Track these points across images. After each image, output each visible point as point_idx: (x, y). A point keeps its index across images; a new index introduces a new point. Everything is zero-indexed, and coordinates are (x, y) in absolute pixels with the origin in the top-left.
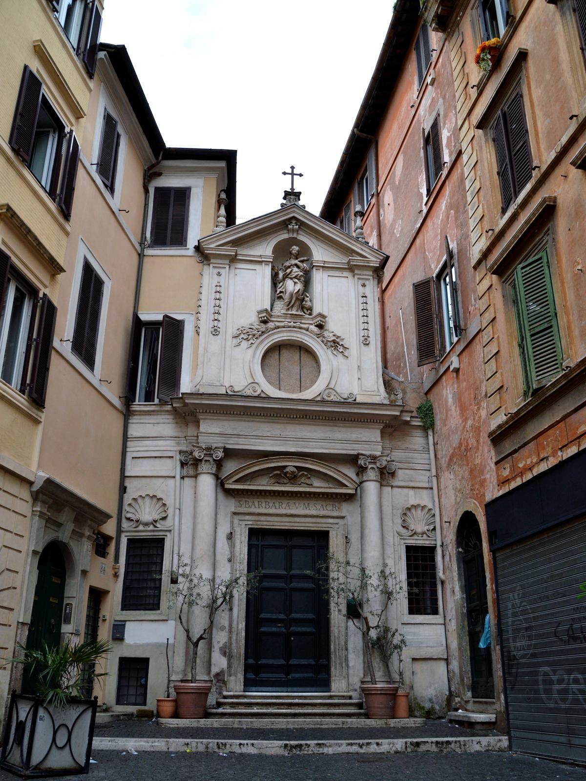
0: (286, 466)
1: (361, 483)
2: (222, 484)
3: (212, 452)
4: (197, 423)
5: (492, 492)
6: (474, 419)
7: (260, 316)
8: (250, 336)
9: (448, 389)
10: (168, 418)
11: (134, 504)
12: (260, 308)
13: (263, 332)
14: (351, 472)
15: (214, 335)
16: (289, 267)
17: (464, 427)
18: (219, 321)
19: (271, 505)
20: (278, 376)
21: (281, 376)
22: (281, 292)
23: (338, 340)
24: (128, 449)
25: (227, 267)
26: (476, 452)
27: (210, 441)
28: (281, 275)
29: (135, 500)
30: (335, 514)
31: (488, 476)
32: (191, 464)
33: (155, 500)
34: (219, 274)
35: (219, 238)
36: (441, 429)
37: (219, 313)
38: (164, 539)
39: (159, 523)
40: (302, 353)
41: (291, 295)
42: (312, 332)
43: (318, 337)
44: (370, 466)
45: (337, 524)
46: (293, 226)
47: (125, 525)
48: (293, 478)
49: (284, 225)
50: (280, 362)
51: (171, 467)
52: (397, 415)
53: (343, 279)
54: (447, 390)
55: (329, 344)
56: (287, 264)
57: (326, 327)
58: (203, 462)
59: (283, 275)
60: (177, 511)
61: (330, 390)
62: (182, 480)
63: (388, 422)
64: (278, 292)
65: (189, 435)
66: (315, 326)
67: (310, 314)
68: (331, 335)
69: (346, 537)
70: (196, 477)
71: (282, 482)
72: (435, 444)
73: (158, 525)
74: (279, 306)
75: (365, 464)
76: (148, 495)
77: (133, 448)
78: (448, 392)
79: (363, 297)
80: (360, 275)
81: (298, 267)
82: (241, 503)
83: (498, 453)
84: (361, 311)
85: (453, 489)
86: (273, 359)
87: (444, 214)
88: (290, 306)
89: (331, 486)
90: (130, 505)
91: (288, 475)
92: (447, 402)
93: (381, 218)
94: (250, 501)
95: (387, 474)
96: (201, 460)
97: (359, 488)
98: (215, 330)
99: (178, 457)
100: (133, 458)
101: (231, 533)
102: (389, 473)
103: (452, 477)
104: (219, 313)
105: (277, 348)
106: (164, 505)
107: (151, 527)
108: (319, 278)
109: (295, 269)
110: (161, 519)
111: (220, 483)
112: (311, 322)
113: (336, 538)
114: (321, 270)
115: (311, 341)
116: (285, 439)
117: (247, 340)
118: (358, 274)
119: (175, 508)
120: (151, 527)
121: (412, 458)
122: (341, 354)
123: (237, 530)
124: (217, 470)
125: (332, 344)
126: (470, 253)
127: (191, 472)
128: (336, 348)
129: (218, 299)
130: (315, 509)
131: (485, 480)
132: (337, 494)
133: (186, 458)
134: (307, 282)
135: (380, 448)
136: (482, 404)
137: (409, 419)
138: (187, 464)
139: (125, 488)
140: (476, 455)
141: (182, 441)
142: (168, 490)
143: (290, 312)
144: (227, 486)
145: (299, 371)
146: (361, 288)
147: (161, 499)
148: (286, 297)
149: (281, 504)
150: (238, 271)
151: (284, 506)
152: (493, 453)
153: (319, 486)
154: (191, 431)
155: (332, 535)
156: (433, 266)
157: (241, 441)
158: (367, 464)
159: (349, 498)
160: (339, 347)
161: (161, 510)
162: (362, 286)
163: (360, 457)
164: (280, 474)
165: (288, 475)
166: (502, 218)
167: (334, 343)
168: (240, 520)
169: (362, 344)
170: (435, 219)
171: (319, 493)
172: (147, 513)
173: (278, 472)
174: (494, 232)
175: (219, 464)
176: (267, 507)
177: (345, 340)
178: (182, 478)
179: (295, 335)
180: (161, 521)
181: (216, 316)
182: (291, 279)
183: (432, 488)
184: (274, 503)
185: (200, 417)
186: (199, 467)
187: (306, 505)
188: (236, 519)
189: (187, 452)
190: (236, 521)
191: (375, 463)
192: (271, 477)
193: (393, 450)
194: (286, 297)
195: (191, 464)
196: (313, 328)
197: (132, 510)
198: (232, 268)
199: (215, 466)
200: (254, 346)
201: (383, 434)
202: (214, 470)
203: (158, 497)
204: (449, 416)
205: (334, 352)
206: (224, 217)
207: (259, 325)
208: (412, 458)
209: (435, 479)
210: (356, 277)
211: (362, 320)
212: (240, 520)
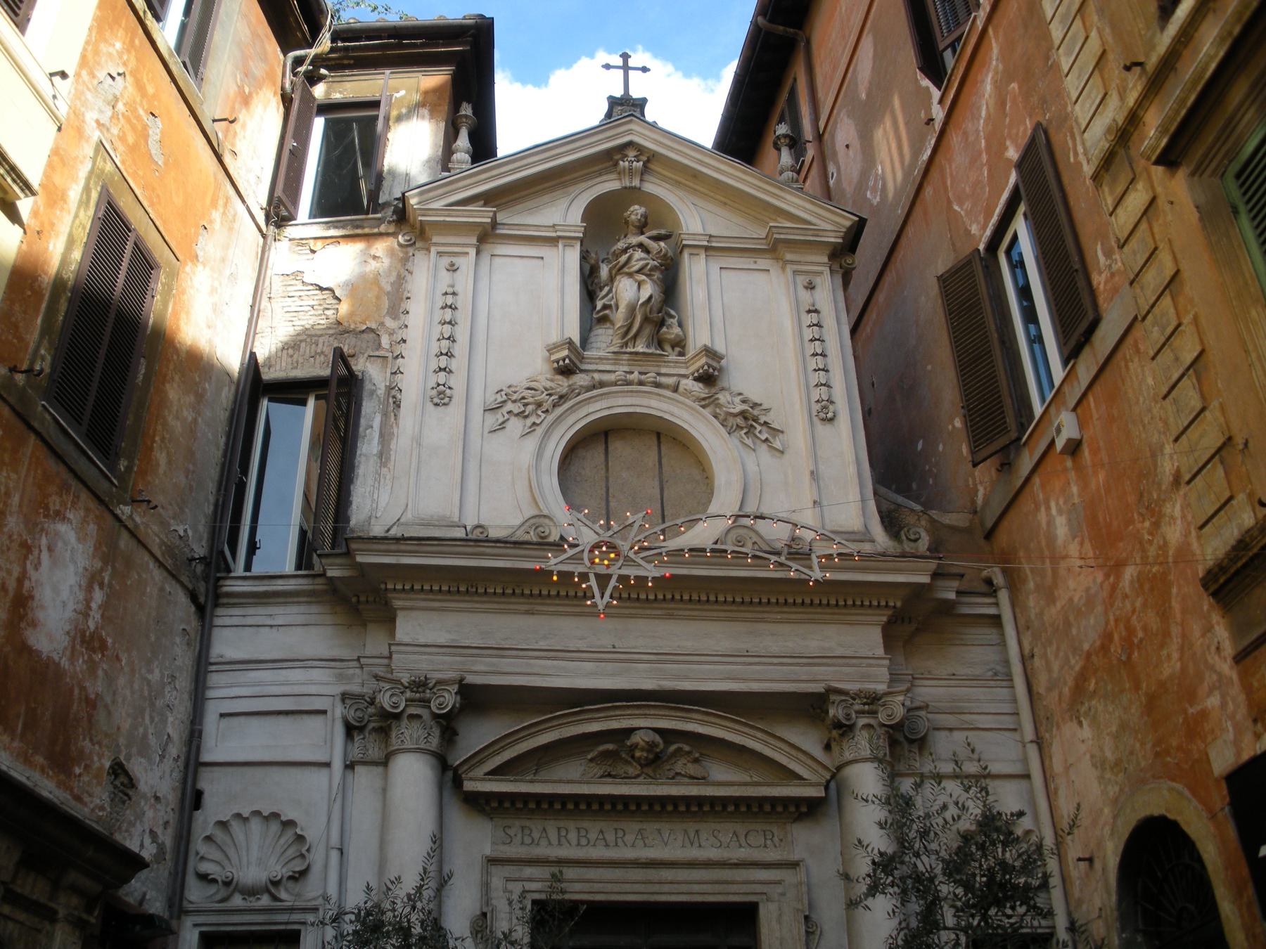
0: (630, 731)
1: (839, 768)
2: (457, 782)
3: (428, 694)
4: (388, 620)
5: (1237, 743)
6: (1144, 558)
7: (554, 357)
8: (530, 408)
9: (1053, 504)
10: (312, 612)
11: (220, 835)
12: (555, 338)
13: (561, 397)
14: (808, 739)
15: (437, 405)
16: (625, 251)
17: (1114, 588)
18: (451, 371)
19: (593, 836)
20: (604, 503)
21: (612, 504)
22: (605, 307)
23: (756, 412)
24: (211, 694)
25: (473, 252)
26: (1162, 645)
27: (424, 666)
28: (604, 271)
29: (223, 825)
30: (772, 855)
31: (1213, 701)
32: (374, 729)
33: (275, 827)
34: (453, 268)
35: (453, 187)
36: (1041, 614)
37: (449, 355)
38: (299, 931)
39: (286, 890)
40: (663, 448)
41: (632, 310)
42: (687, 393)
43: (703, 407)
44: (862, 721)
45: (779, 882)
46: (630, 162)
47: (195, 893)
48: (654, 761)
49: (608, 160)
50: (607, 470)
51: (320, 739)
52: (922, 585)
53: (757, 274)
54: (1048, 508)
55: (731, 421)
56: (621, 245)
57: (723, 383)
58: (405, 721)
59: (610, 271)
60: (335, 855)
61: (741, 531)
62: (349, 773)
63: (899, 604)
64: (599, 306)
65: (368, 653)
66: (696, 379)
67: (682, 354)
68: (737, 399)
69: (807, 918)
70: (385, 762)
71: (621, 772)
72: (1026, 659)
73: (283, 895)
74: (603, 338)
75: (848, 716)
76: (257, 813)
77: (226, 691)
78: (1054, 511)
79: (809, 312)
80: (798, 263)
81: (647, 250)
82: (511, 832)
83: (1237, 630)
84: (807, 344)
85: (1094, 765)
86: (592, 459)
87: (992, 102)
88: (629, 337)
89: (756, 779)
90: (209, 839)
91: (638, 754)
92: (1051, 539)
93: (831, 182)
94: (536, 826)
95: (906, 745)
96: (397, 717)
97: (833, 785)
98: (440, 393)
99: (339, 711)
100: (222, 715)
101: (484, 915)
102: (911, 742)
103: (1086, 732)
104: (449, 355)
105: (600, 435)
106: (300, 838)
107: (265, 901)
108: (698, 277)
109: (639, 254)
110: (290, 878)
111: (450, 776)
112: (683, 371)
113: (779, 921)
114: (703, 256)
115: (686, 415)
116: (627, 658)
117: (522, 415)
118: (792, 262)
119: (328, 848)
120: (265, 901)
121: (969, 701)
122: (764, 446)
123: (501, 904)
124: (441, 744)
125: (740, 421)
126: (1076, 154)
127: (375, 752)
128: (750, 431)
129: (450, 323)
130: (714, 842)
131: (1204, 714)
132: (774, 801)
133: (359, 714)
134: (669, 278)
135: (883, 673)
136: (1167, 509)
137: (952, 596)
138: (361, 729)
139: (198, 795)
140: (1165, 652)
141: (351, 671)
142: (307, 799)
143: (629, 350)
144: (469, 786)
145: (657, 491)
146: (805, 296)
147: (290, 824)
148: (619, 317)
149: (620, 834)
150: (497, 260)
151: (629, 838)
152: (1222, 632)
153: (724, 779)
154: (375, 643)
155: (767, 914)
156: (974, 229)
157: (506, 664)
158: (854, 716)
159: (808, 810)
160: (759, 428)
161: (291, 852)
162: (806, 288)
163: (833, 697)
164: (613, 749)
165: (638, 754)
166: (1163, 28)
167: (746, 418)
168: (508, 880)
169: (815, 419)
170: (969, 126)
171: (725, 801)
172: (255, 859)
173: (610, 747)
174: (1144, 70)
175: (448, 725)
176: (584, 841)
177: (772, 413)
178: (350, 766)
179: (645, 401)
180: (290, 884)
181: (443, 361)
182: (630, 275)
183: (1027, 776)
184: (601, 832)
185: (397, 603)
186: (394, 734)
187: (692, 835)
188: (498, 878)
189: (362, 696)
190: (497, 882)
191: (873, 713)
192: (591, 760)
193: (918, 682)
194: (619, 317)
195: (371, 728)
196: (688, 384)
197: (214, 853)
198: (485, 258)
199: (436, 732)
200: (539, 431)
201: (889, 640)
202: (435, 742)
203: (284, 818)
204: (1062, 572)
205: (749, 442)
206: (467, 152)
207: (552, 380)
208: (969, 701)
209: (1033, 752)
210: (789, 269)
211: (812, 363)
212: (508, 880)
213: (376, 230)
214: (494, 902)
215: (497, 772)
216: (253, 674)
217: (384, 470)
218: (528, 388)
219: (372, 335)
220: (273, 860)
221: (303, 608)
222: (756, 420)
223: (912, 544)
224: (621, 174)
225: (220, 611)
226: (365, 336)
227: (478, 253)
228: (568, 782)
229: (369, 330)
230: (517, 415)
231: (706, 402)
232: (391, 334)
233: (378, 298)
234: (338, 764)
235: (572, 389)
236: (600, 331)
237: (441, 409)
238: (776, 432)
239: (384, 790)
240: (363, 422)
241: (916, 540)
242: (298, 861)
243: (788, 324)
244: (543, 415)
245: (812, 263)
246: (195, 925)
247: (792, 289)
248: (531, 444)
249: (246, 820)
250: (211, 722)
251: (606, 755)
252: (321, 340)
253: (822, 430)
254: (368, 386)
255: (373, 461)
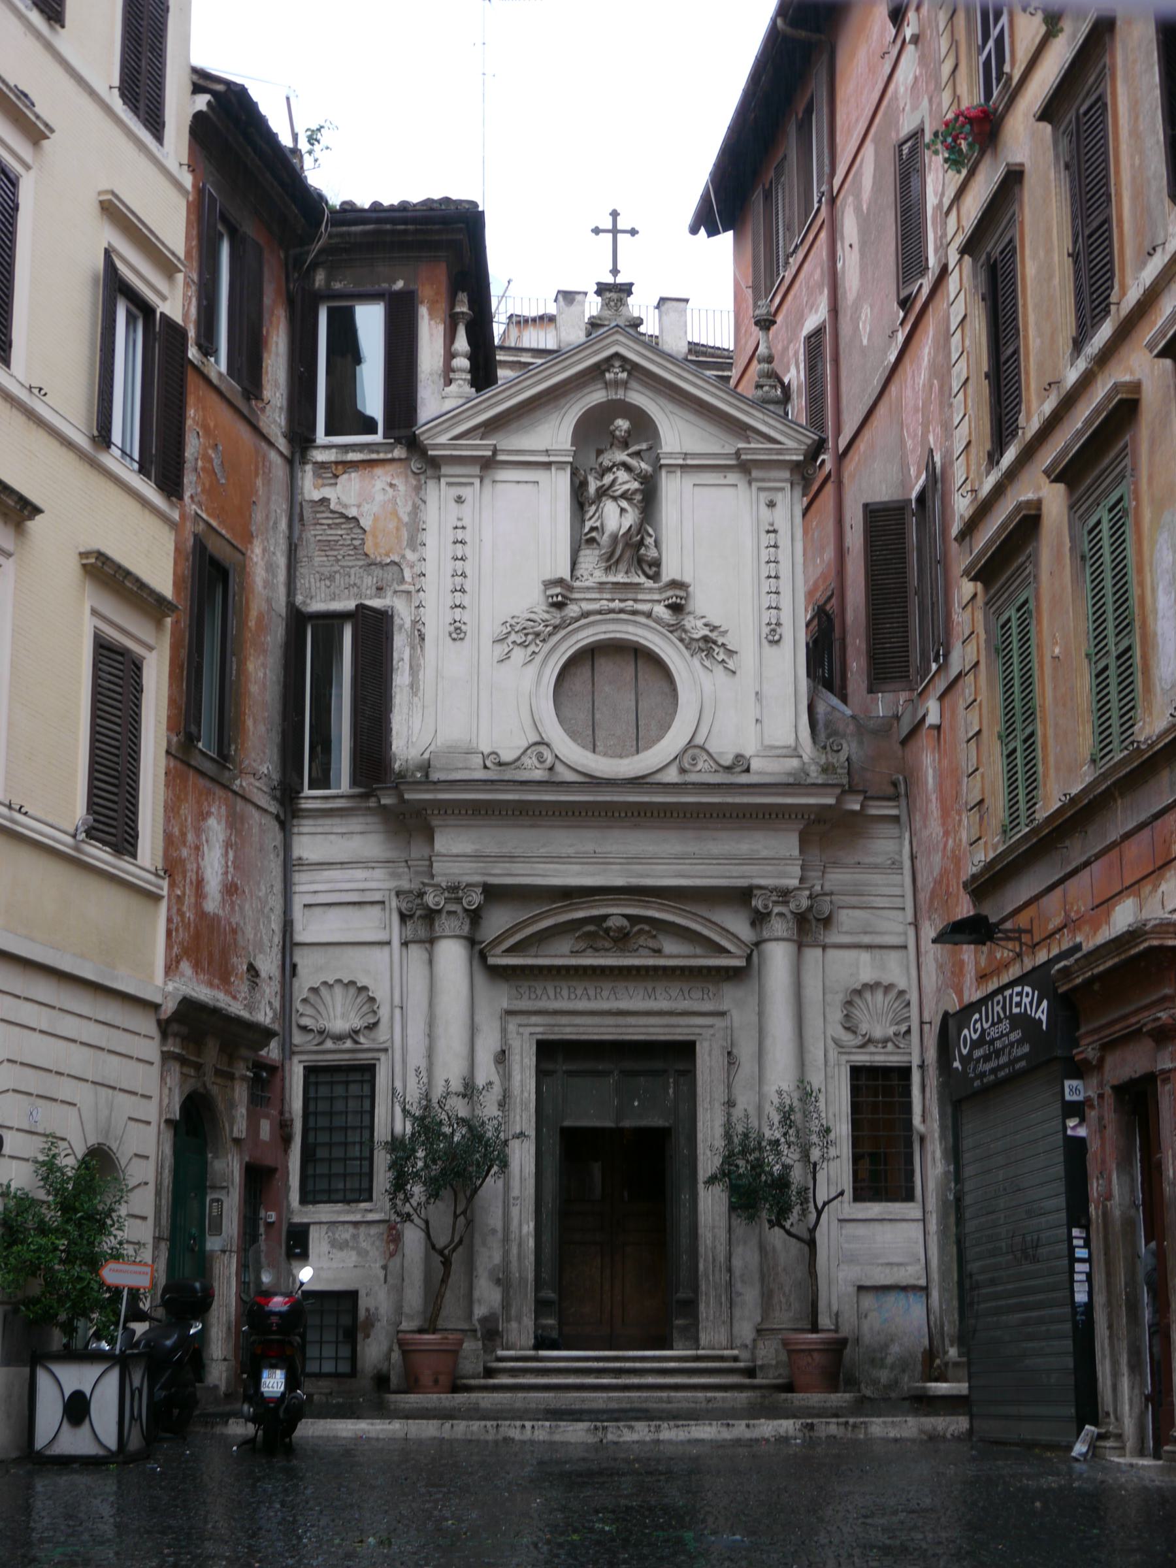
2: (483, 957)
3: (461, 894)
4: (429, 836)
7: (549, 592)
8: (530, 637)
11: (313, 998)
15: (454, 639)
18: (464, 607)
22: (593, 529)
24: (297, 888)
29: (314, 990)
32: (420, 916)
33: (352, 991)
40: (639, 664)
42: (658, 621)
43: (671, 632)
47: (298, 1038)
55: (695, 645)
58: (444, 915)
60: (397, 1012)
66: (667, 606)
68: (700, 623)
73: (362, 1040)
76: (339, 981)
77: (306, 886)
80: (763, 480)
90: (305, 1000)
96: (439, 911)
98: (456, 629)
100: (305, 906)
101: (503, 1052)
106: (372, 1000)
107: (349, 1044)
108: (674, 492)
109: (622, 475)
110: (366, 1027)
111: (478, 952)
114: (679, 474)
116: (604, 861)
119: (392, 1007)
120: (349, 1044)
122: (720, 667)
125: (702, 644)
127: (422, 933)
128: (709, 653)
129: (462, 559)
133: (410, 905)
134: (647, 499)
138: (411, 916)
141: (401, 870)
142: (374, 970)
150: (500, 486)
154: (418, 850)
160: (717, 650)
161: (365, 1008)
164: (595, 932)
168: (520, 1025)
172: (340, 1016)
175: (475, 917)
178: (405, 944)
179: (623, 627)
180: (366, 1032)
182: (615, 499)
188: (512, 1025)
189: (411, 892)
190: (512, 1027)
194: (605, 540)
197: (309, 1011)
198: (487, 481)
200: (538, 659)
203: (359, 985)
205: (707, 663)
206: (466, 356)
207: (548, 612)
210: (755, 485)
212: (520, 1025)
213: (389, 456)
214: (510, 1042)
215: (510, 951)
216: (326, 873)
217: (416, 699)
218: (529, 620)
219: (395, 568)
220: (352, 1015)
221: (361, 819)
222: (715, 643)
223: (835, 754)
224: (607, 385)
225: (295, 822)
226: (389, 568)
227: (481, 482)
228: (562, 956)
229: (393, 563)
230: (520, 644)
231: (674, 628)
232: (412, 567)
233: (398, 529)
234: (396, 943)
235: (563, 620)
236: (588, 552)
237: (458, 643)
238: (731, 653)
239: (431, 962)
240: (395, 655)
241: (838, 751)
242: (370, 1015)
243: (748, 542)
244: (541, 644)
245: (775, 480)
246: (300, 1062)
247: (755, 507)
248: (532, 670)
249: (331, 986)
250: (298, 913)
251: (589, 935)
252: (353, 571)
253: (768, 649)
254: (397, 621)
255: (406, 690)
